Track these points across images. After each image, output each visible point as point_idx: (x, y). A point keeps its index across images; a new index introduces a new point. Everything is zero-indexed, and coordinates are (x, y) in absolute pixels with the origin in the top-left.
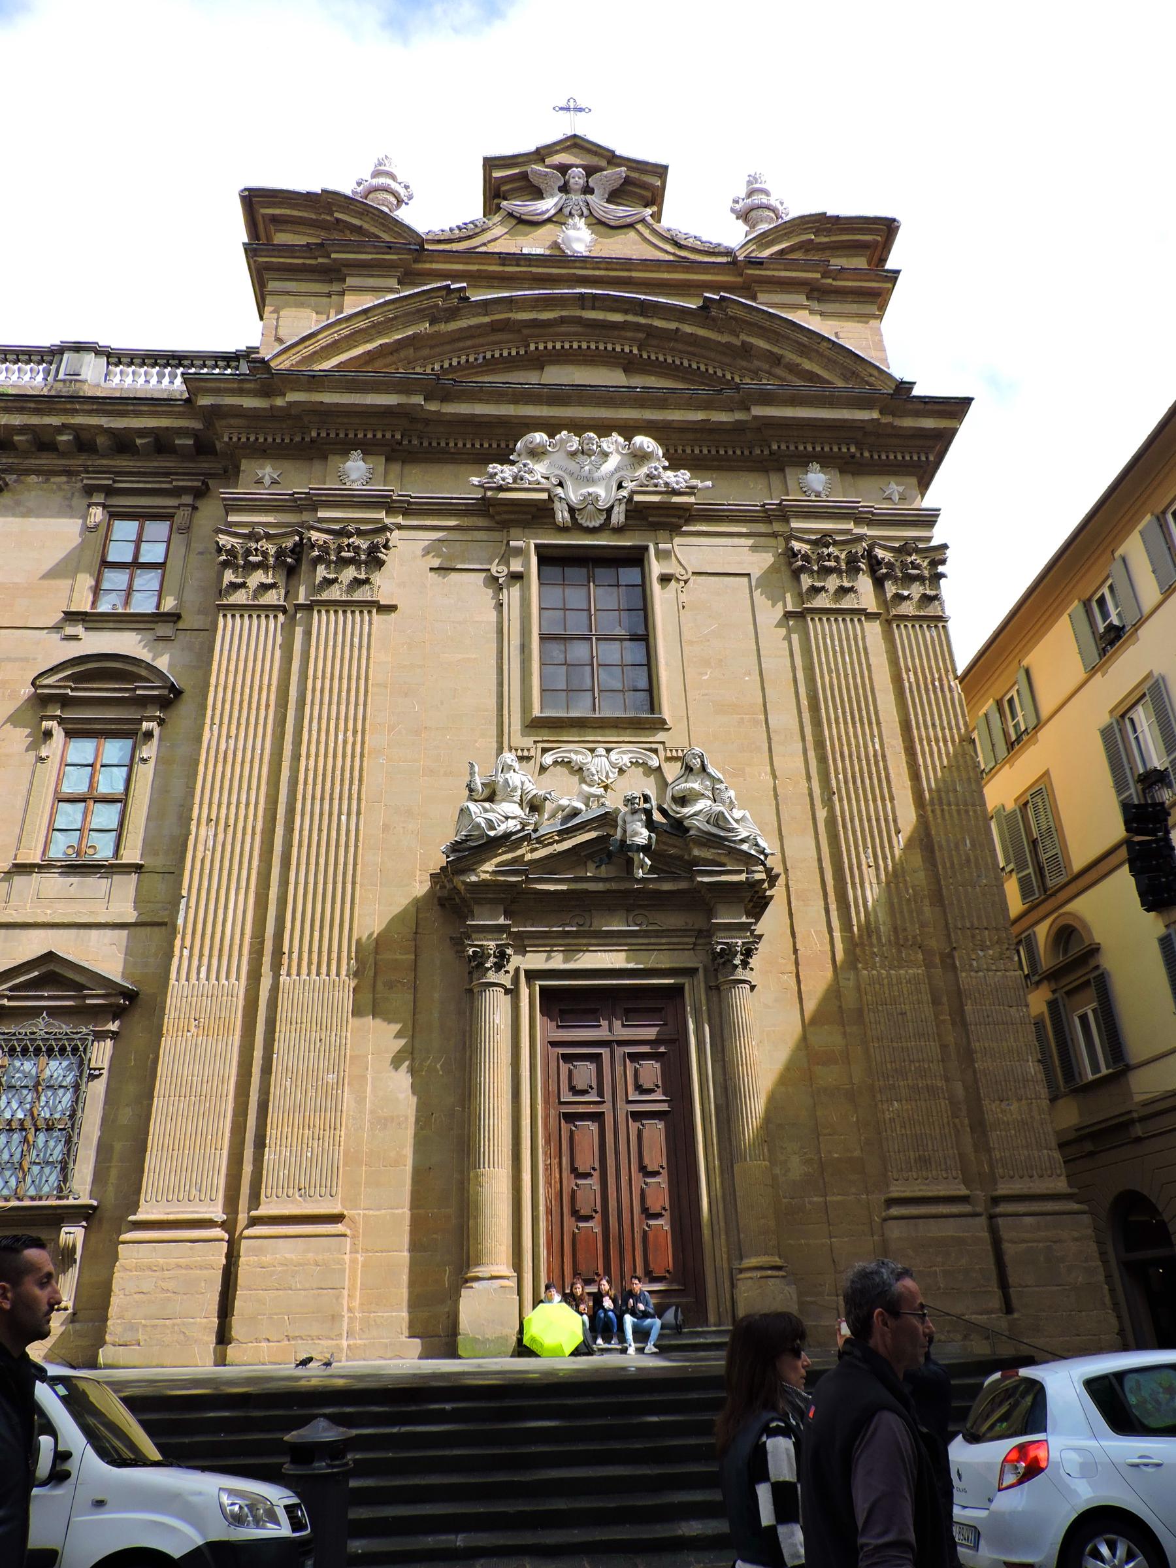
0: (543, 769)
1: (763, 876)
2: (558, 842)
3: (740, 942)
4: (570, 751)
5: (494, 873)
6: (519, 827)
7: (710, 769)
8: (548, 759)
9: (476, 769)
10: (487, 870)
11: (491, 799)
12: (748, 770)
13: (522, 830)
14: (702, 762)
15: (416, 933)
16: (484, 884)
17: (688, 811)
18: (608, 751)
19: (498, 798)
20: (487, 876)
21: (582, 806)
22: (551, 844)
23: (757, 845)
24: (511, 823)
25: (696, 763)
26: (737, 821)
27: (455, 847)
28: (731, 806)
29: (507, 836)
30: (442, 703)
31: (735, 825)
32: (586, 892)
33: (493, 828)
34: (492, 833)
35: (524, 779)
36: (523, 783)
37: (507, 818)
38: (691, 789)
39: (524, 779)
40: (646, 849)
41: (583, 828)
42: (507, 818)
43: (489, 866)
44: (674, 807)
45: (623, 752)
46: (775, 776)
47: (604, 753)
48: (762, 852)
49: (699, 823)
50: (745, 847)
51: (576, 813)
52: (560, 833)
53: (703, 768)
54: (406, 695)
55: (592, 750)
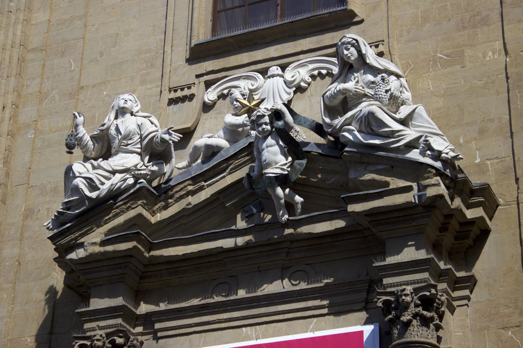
0: (207, 107)
1: (442, 190)
2: (193, 193)
3: (409, 289)
4: (238, 79)
5: (103, 243)
6: (131, 181)
7: (372, 59)
8: (211, 95)
9: (80, 120)
10: (93, 241)
11: (107, 155)
12: (468, 52)
13: (136, 183)
14: (359, 51)
15: (51, 333)
16: (91, 260)
17: (339, 121)
18: (283, 68)
19: (113, 151)
20: (97, 249)
21: (223, 143)
22: (181, 197)
23: (430, 148)
24: (118, 176)
25: (352, 53)
26: (404, 122)
27: (59, 219)
28: (395, 102)
29: (114, 195)
30: (101, 56)
31: (396, 126)
32: (221, 251)
33: (92, 186)
34: (94, 195)
35: (146, 121)
36: (139, 126)
37: (114, 172)
38: (344, 92)
39: (140, 120)
40: (282, 180)
41: (224, 171)
42: (114, 172)
43: (97, 235)
44: (327, 120)
45: (302, 65)
46: (506, 53)
47: (279, 71)
48: (437, 155)
49: (353, 134)
50: (414, 155)
51: (212, 151)
52: (195, 179)
53: (361, 56)
54: (63, 54)
55: (264, 72)
